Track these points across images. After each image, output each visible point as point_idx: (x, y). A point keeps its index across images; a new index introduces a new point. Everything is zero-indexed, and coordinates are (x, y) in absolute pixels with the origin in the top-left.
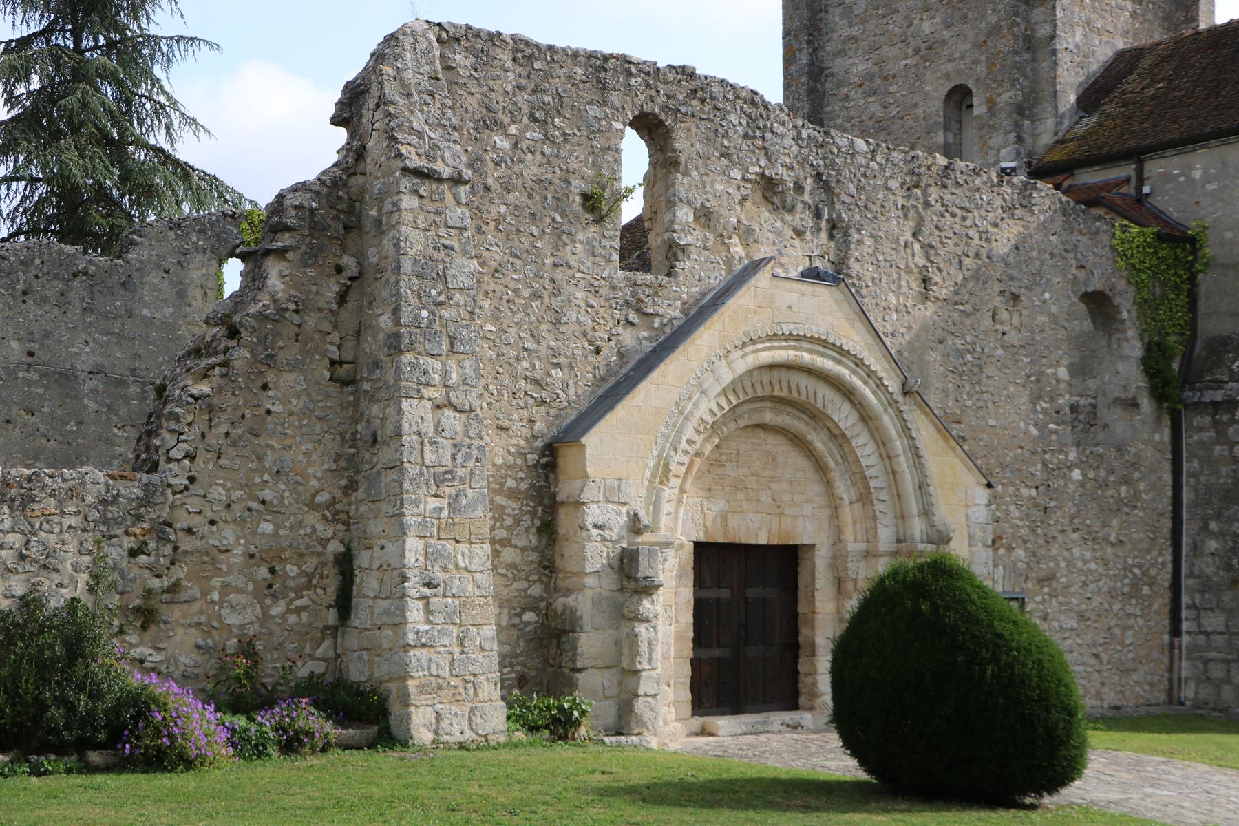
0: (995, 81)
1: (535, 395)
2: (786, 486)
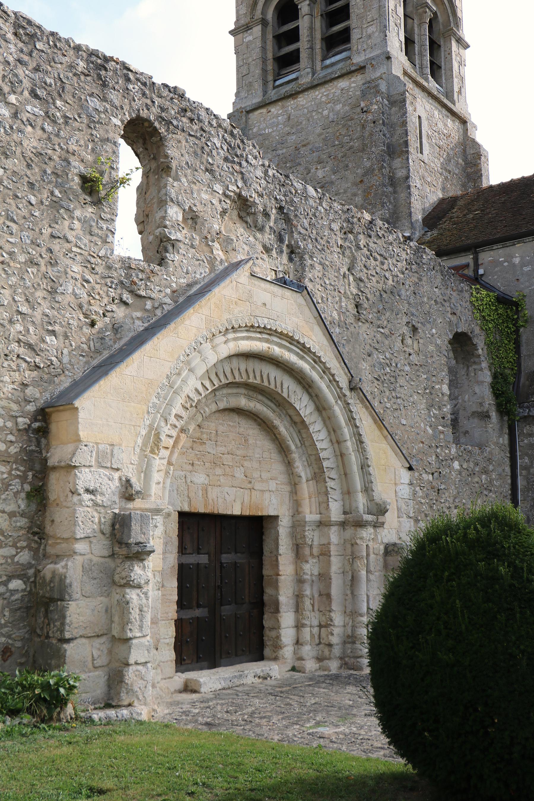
1: (28, 359)
2: (256, 465)
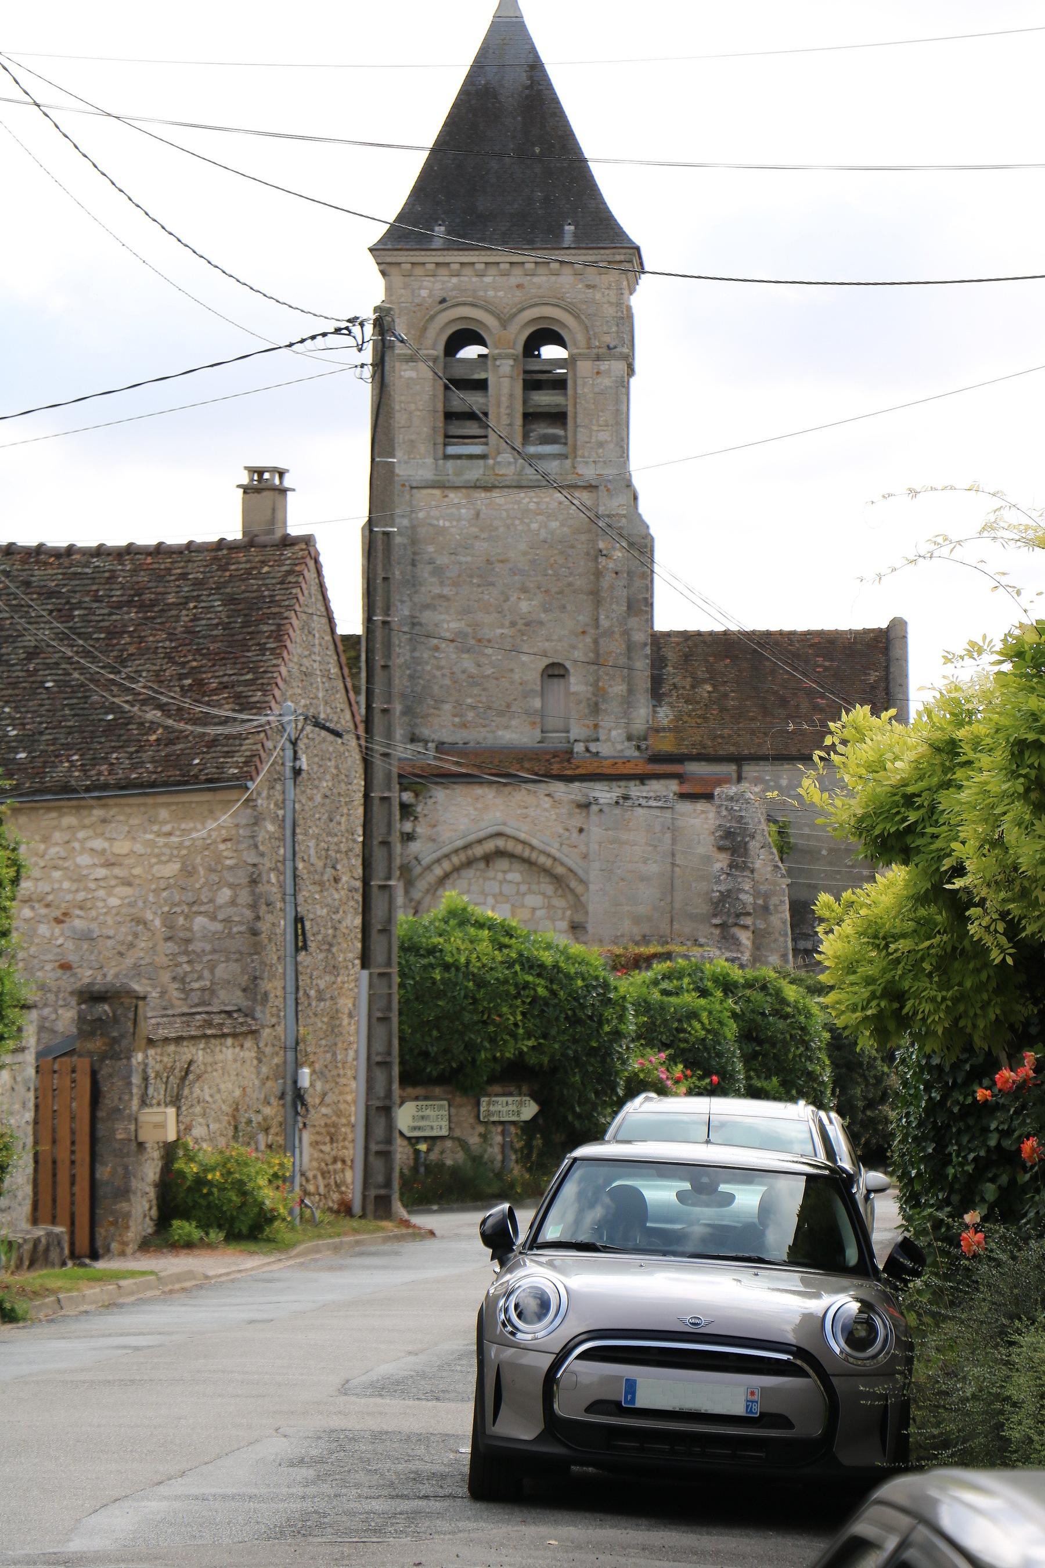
0: (607, 674)
